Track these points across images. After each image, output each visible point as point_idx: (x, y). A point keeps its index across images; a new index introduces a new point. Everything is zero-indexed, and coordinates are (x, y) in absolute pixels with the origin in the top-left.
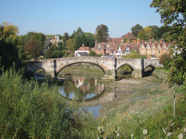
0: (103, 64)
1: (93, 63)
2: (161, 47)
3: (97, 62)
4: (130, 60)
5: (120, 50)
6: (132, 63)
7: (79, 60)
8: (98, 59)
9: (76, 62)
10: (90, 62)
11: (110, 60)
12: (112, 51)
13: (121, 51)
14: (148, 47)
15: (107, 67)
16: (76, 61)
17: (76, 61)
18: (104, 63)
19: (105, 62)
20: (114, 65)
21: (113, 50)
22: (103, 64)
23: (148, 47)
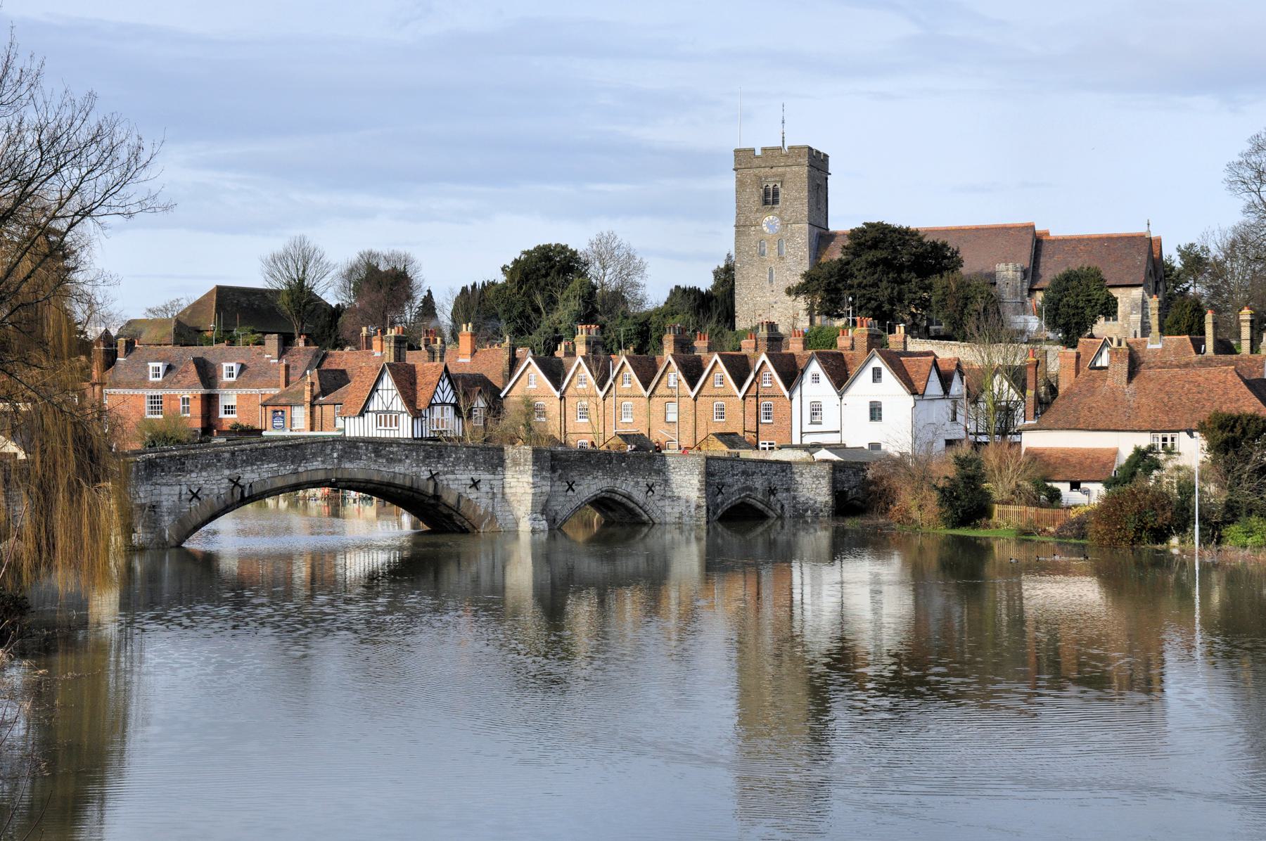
0: (473, 495)
1: (408, 483)
2: (692, 387)
3: (432, 477)
4: (629, 467)
5: (389, 395)
6: (642, 482)
7: (399, 469)
8: (440, 456)
9: (293, 480)
10: (387, 478)
11: (516, 463)
12: (277, 407)
13: (398, 404)
14: (581, 376)
15: (493, 518)
16: (295, 472)
17: (295, 472)
18: (475, 484)
19: (484, 476)
20: (544, 498)
21: (283, 401)
22: (473, 495)
23: (581, 376)
